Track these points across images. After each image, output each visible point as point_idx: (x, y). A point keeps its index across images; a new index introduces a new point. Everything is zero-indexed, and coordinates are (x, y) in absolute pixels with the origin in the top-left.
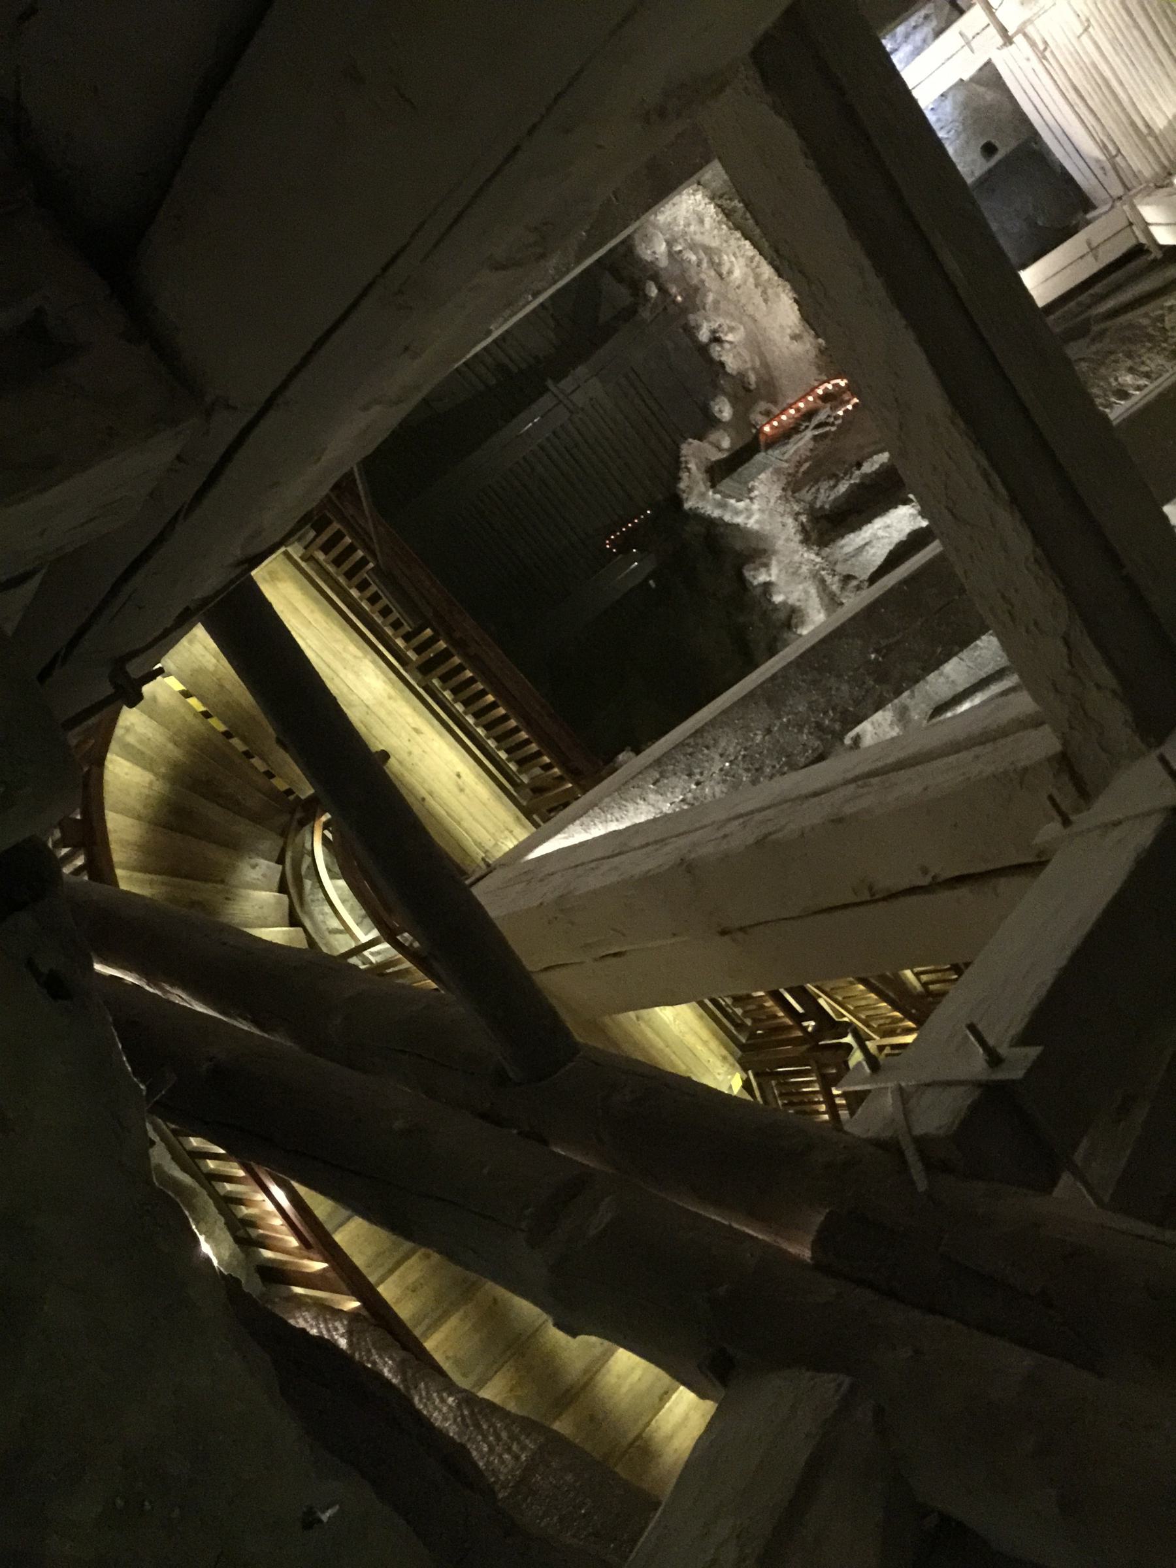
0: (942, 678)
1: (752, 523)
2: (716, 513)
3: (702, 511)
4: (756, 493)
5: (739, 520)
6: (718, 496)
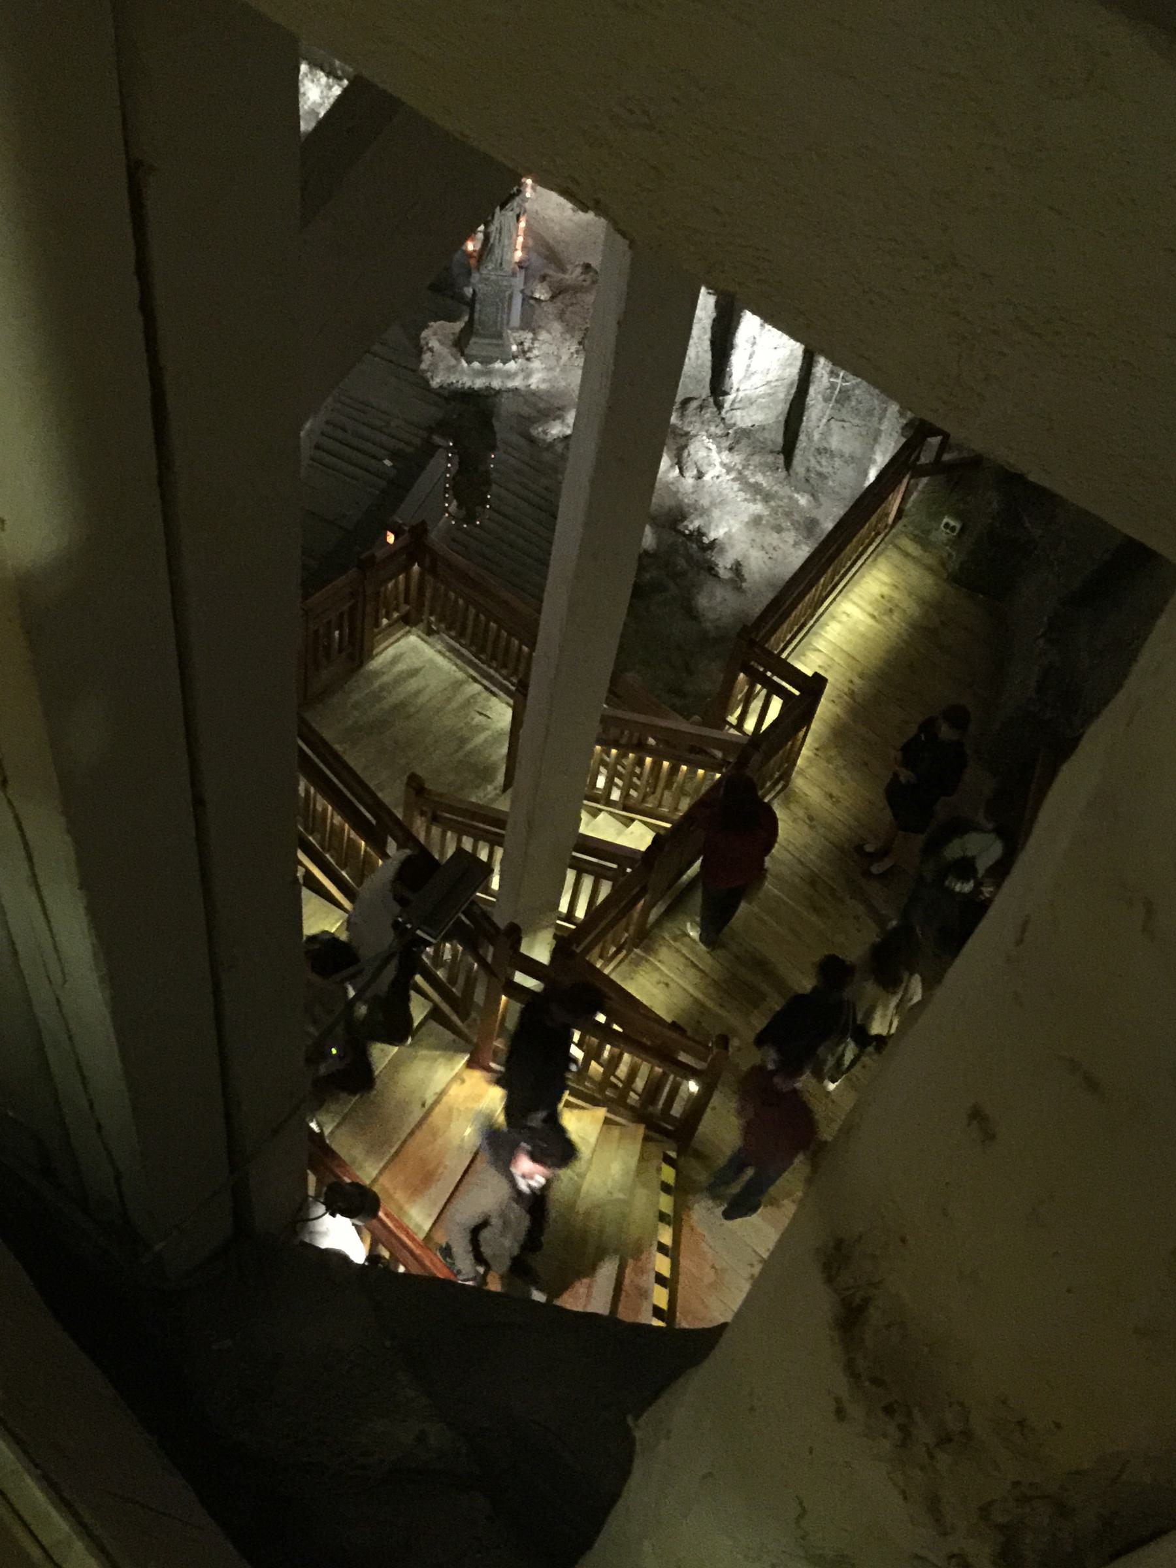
0: (836, 459)
1: (536, 381)
2: (479, 383)
3: (460, 386)
4: (536, 352)
5: (517, 383)
6: (476, 365)
